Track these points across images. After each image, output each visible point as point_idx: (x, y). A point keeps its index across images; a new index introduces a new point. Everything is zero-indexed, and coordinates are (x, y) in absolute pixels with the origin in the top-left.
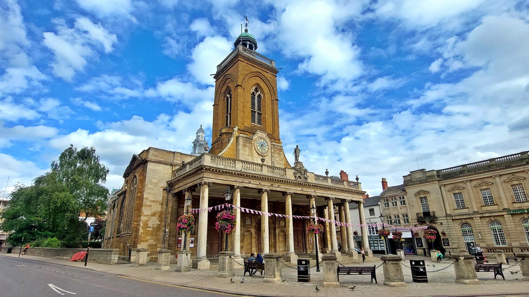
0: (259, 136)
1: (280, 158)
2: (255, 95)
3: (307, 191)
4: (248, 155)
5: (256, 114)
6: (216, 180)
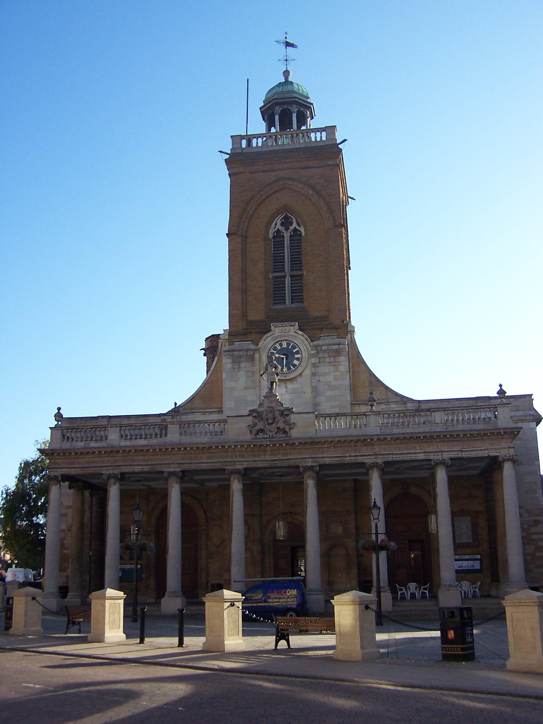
0: (276, 334)
1: (338, 373)
2: (283, 236)
3: (288, 459)
4: (246, 388)
5: (288, 280)
6: (69, 470)
